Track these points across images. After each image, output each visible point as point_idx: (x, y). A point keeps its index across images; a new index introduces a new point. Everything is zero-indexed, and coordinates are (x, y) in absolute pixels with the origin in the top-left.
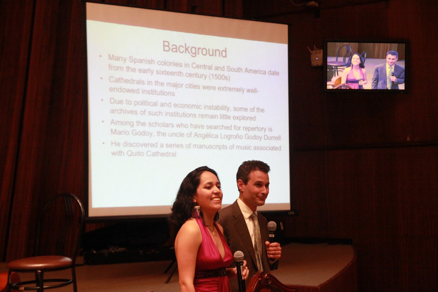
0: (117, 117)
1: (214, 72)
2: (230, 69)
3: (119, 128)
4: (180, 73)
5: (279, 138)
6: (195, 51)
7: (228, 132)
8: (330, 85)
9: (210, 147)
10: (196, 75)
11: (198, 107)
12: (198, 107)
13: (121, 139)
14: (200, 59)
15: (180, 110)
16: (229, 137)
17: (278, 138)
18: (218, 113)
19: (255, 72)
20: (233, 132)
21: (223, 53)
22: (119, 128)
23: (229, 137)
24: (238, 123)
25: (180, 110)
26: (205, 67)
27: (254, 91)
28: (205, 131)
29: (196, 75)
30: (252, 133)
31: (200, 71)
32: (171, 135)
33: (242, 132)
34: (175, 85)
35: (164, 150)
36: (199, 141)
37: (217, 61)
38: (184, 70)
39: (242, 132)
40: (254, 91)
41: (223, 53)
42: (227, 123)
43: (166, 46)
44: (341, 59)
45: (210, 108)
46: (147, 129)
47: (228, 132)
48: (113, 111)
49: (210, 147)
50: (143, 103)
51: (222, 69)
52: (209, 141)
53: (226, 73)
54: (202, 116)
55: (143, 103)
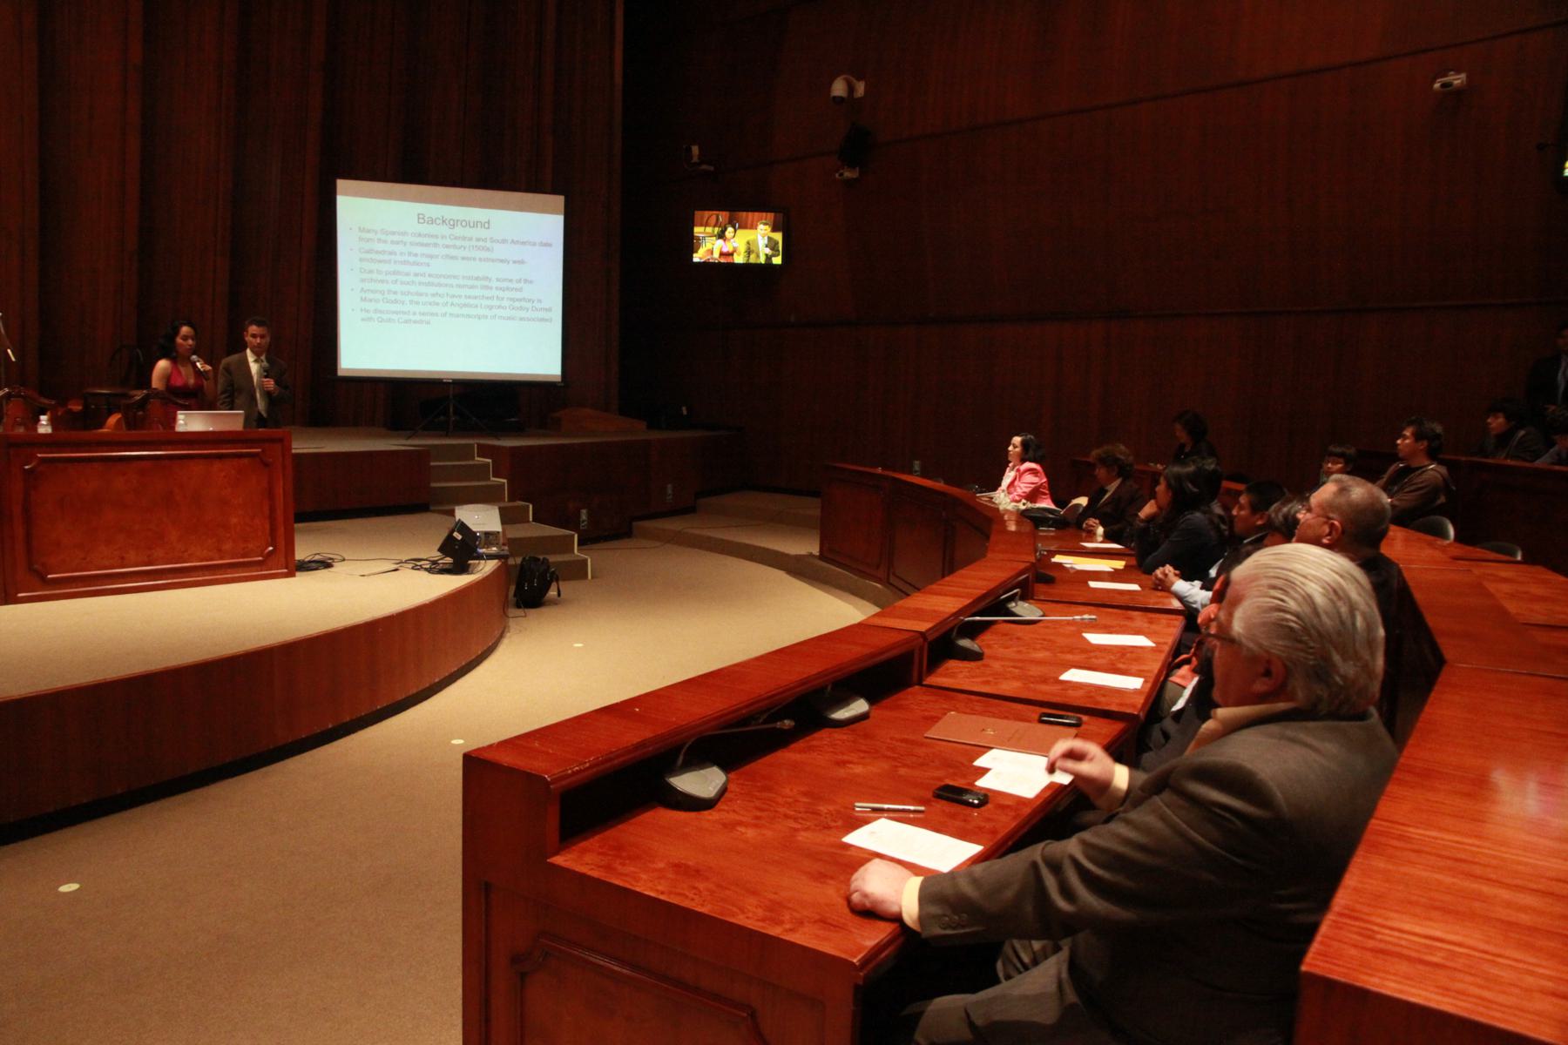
0: (367, 286)
1: (474, 243)
2: (492, 240)
3: (370, 296)
4: (436, 245)
5: (549, 310)
6: (454, 224)
7: (489, 302)
8: (697, 258)
9: (469, 316)
10: (454, 247)
11: (455, 277)
12: (455, 277)
13: (370, 306)
14: (459, 231)
15: (436, 281)
16: (491, 308)
17: (549, 310)
18: (479, 283)
19: (524, 243)
20: (495, 302)
21: (486, 225)
22: (370, 296)
23: (491, 308)
24: (501, 294)
25: (436, 281)
26: (464, 238)
27: (522, 262)
28: (463, 301)
29: (454, 247)
30: (517, 304)
31: (458, 243)
32: (424, 304)
33: (506, 303)
34: (431, 256)
35: (417, 317)
36: (456, 310)
37: (482, 233)
38: (440, 241)
39: (506, 303)
40: (522, 262)
41: (486, 225)
42: (487, 293)
43: (421, 218)
44: (709, 229)
45: (469, 278)
46: (399, 297)
47: (489, 302)
48: (363, 280)
49: (469, 316)
50: (395, 273)
51: (485, 240)
52: (465, 311)
53: (488, 244)
54: (459, 286)
55: (395, 273)
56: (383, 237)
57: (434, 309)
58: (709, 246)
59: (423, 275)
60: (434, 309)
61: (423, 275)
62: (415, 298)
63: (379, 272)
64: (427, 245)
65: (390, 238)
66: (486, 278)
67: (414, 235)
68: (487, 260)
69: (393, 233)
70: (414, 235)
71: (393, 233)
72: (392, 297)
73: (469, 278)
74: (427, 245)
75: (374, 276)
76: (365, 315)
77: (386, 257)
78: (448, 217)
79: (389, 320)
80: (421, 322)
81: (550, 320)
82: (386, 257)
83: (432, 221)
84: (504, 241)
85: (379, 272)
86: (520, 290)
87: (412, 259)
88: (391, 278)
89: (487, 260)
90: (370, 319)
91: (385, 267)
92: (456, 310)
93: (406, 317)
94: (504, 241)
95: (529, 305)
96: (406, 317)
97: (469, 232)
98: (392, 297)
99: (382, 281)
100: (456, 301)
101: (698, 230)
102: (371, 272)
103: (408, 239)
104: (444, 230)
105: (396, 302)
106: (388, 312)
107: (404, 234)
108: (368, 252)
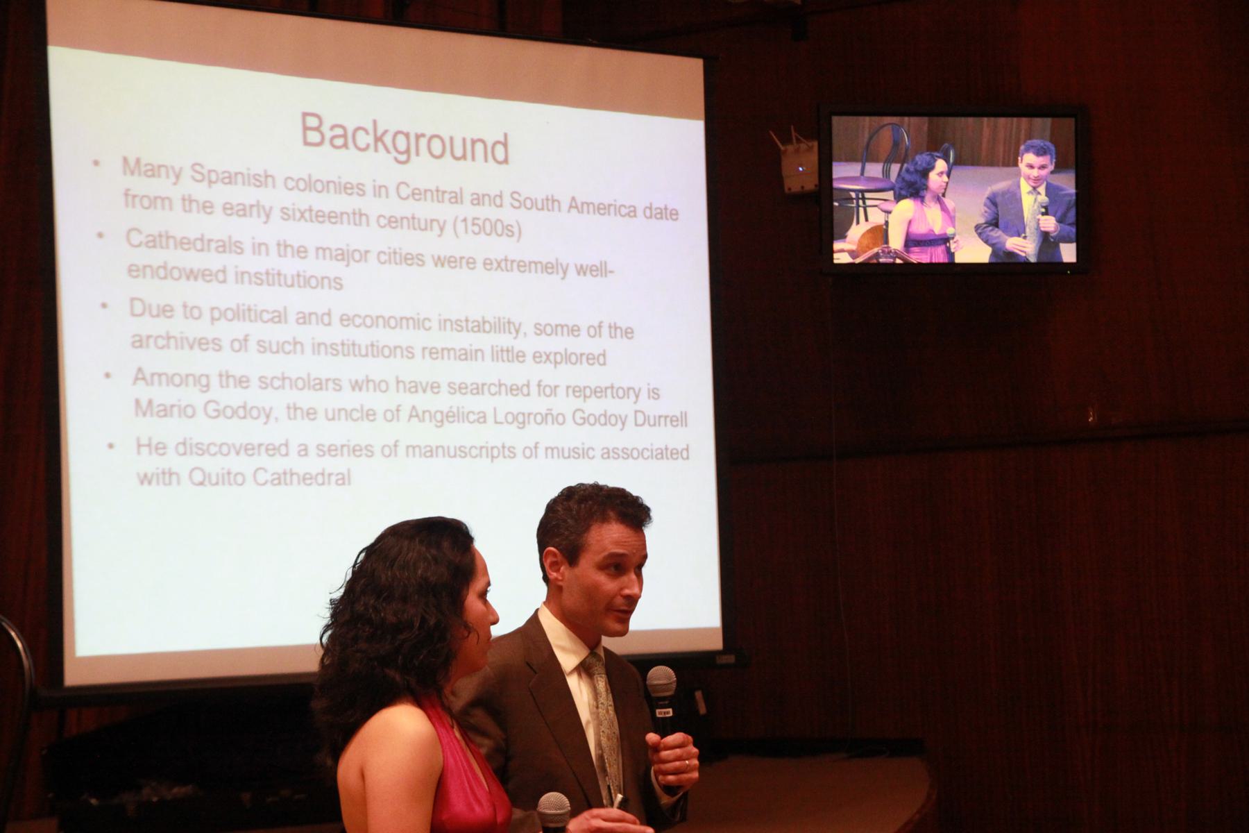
1: (467, 210)
2: (520, 202)
3: (163, 395)
4: (358, 217)
5: (680, 420)
6: (406, 146)
9: (462, 452)
10: (412, 222)
11: (419, 323)
12: (419, 323)
13: (169, 430)
14: (423, 171)
16: (521, 420)
17: (680, 420)
18: (484, 341)
19: (602, 209)
20: (537, 404)
22: (163, 395)
23: (521, 420)
24: (547, 374)
25: (362, 336)
27: (600, 270)
28: (444, 402)
29: (412, 222)
30: (594, 406)
31: (425, 210)
33: (564, 404)
34: (344, 256)
35: (312, 464)
36: (426, 434)
38: (373, 206)
39: (564, 404)
40: (600, 270)
43: (312, 128)
44: (874, 170)
45: (460, 325)
46: (255, 396)
49: (462, 452)
50: (240, 313)
51: (496, 200)
52: (456, 434)
53: (507, 214)
54: (434, 353)
55: (240, 313)
56: (201, 192)
57: (360, 433)
58: (876, 217)
59: (325, 318)
60: (360, 433)
61: (325, 318)
62: (307, 399)
63: (191, 312)
64: (333, 217)
65: (221, 194)
66: (507, 326)
67: (294, 184)
68: (504, 264)
69: (230, 178)
70: (294, 184)
71: (230, 178)
72: (233, 396)
73: (460, 325)
74: (333, 217)
75: (178, 325)
76: (151, 463)
77: (213, 261)
78: (389, 123)
79: (229, 478)
80: (322, 478)
81: (680, 454)
82: (213, 261)
83: (344, 138)
84: (550, 203)
85: (191, 312)
86: (598, 359)
87: (290, 266)
88: (228, 331)
89: (504, 264)
90: (168, 476)
91: (206, 295)
92: (426, 434)
93: (277, 464)
94: (550, 203)
95: (624, 407)
96: (277, 464)
97: (448, 174)
98: (233, 396)
99: (201, 343)
100: (424, 401)
101: (844, 173)
102: (165, 311)
103: (274, 197)
104: (376, 167)
105: (244, 412)
106: (225, 449)
107: (262, 180)
108: (154, 241)
